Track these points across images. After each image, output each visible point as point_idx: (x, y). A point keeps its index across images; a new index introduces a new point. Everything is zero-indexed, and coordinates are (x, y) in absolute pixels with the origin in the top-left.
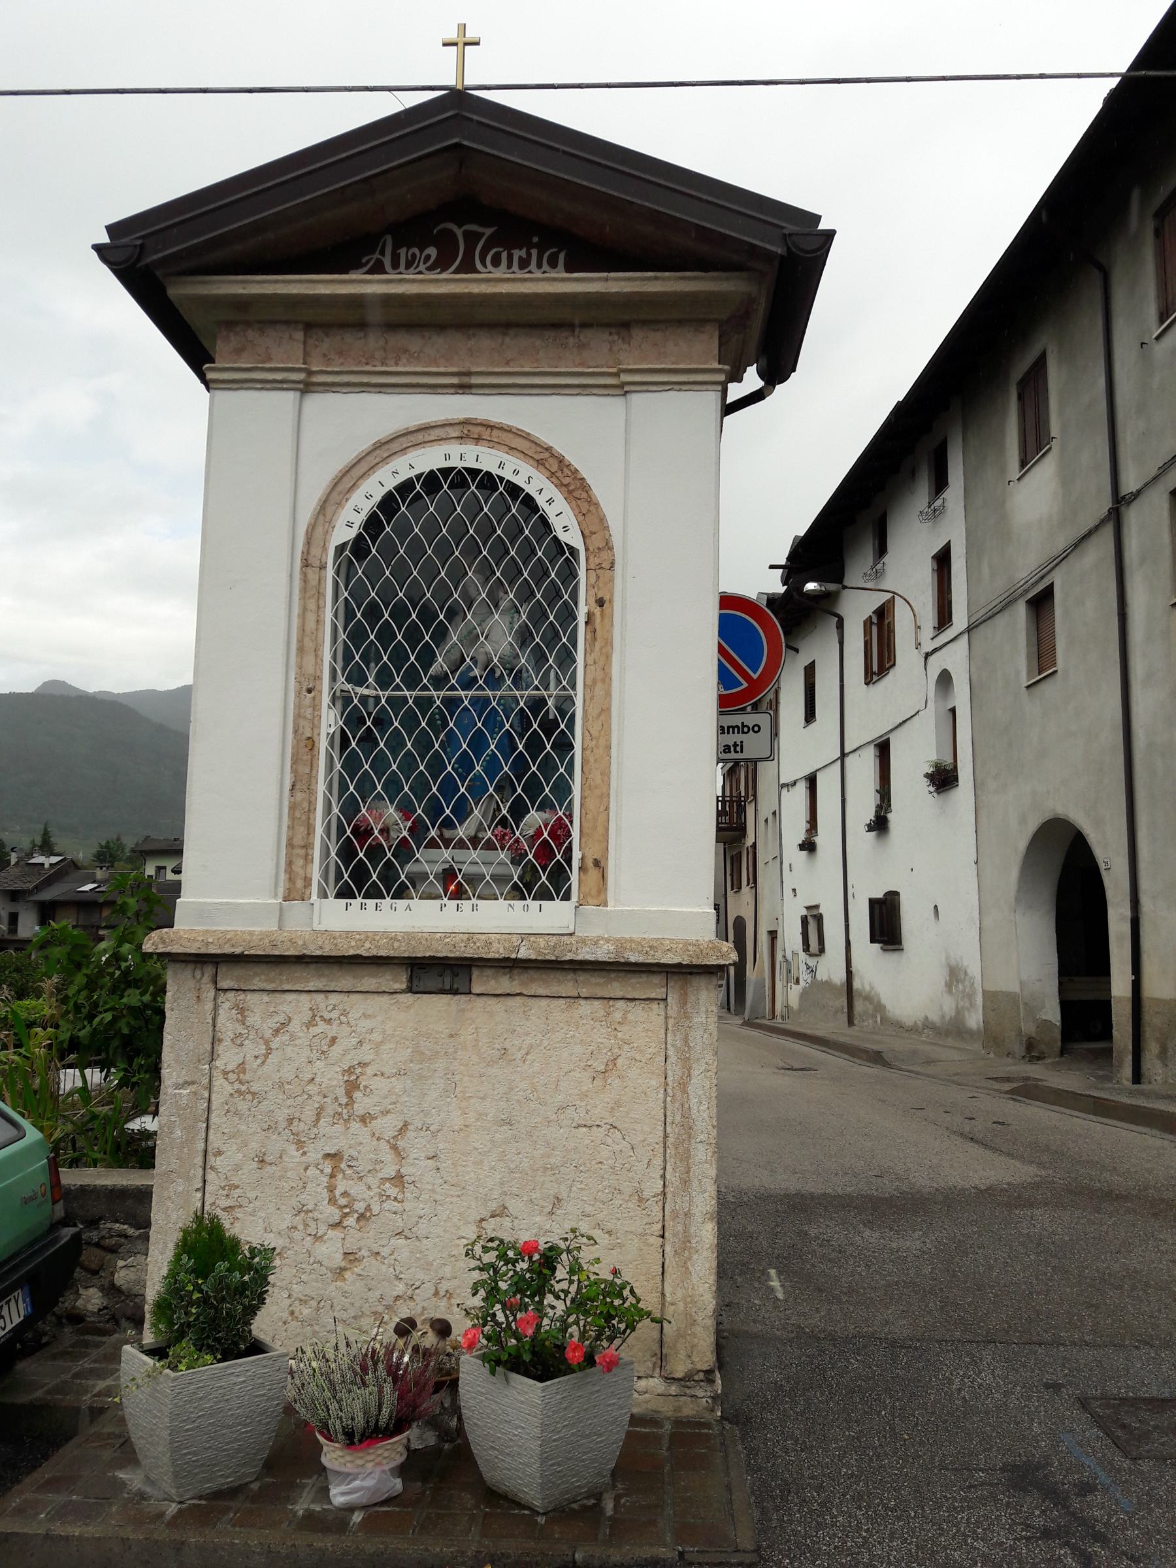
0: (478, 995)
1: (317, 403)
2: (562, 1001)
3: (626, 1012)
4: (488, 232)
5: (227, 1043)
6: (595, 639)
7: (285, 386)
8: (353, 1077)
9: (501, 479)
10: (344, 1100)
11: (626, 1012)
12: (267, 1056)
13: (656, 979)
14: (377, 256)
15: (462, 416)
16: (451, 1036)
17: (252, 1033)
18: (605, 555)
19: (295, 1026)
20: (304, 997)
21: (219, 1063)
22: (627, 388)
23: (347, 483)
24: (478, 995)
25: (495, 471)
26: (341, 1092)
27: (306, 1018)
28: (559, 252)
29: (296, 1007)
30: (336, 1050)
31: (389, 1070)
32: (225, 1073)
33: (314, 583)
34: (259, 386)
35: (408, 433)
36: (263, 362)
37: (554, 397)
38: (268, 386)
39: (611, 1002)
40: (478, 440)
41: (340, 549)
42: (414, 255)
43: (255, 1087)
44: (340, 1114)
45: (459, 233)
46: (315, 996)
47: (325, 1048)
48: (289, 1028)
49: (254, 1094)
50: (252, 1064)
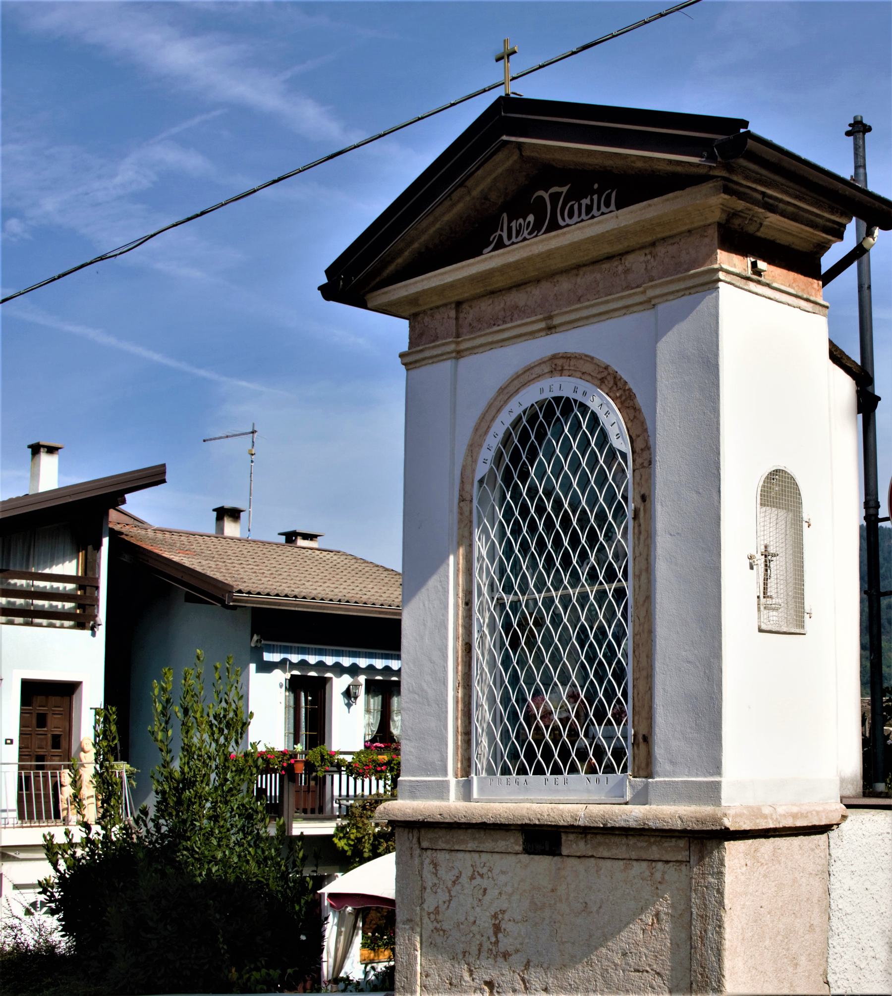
0: (568, 856)
1: (466, 362)
2: (621, 863)
3: (664, 873)
4: (565, 189)
5: (428, 890)
6: (640, 533)
7: (445, 357)
8: (497, 922)
9: (575, 401)
10: (493, 939)
11: (664, 873)
12: (450, 901)
13: (682, 843)
14: (499, 232)
15: (549, 353)
16: (553, 891)
17: (441, 883)
18: (645, 454)
19: (464, 879)
20: (468, 855)
21: (425, 906)
22: (653, 303)
23: (484, 425)
24: (568, 856)
25: (572, 396)
26: (491, 932)
27: (470, 874)
28: (611, 193)
29: (464, 862)
30: (487, 898)
31: (518, 918)
32: (429, 914)
33: (467, 513)
34: (430, 361)
35: (518, 376)
36: (434, 341)
37: (586, 327)
38: (435, 360)
39: (654, 864)
40: (561, 372)
41: (481, 481)
42: (520, 224)
43: (446, 926)
44: (491, 950)
45: (546, 196)
46: (473, 853)
47: (480, 897)
48: (460, 880)
49: (444, 931)
50: (443, 908)
